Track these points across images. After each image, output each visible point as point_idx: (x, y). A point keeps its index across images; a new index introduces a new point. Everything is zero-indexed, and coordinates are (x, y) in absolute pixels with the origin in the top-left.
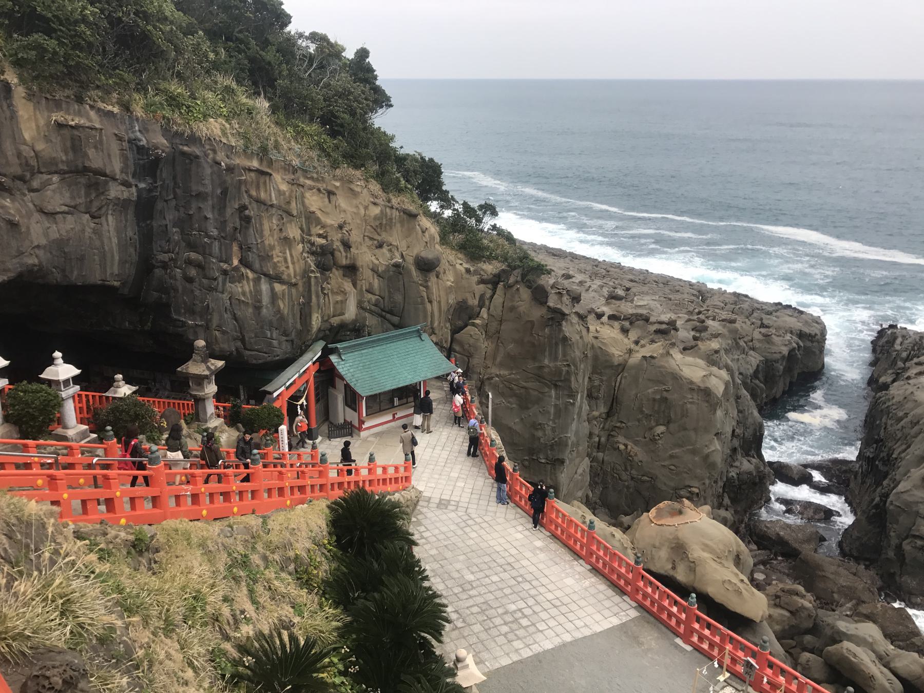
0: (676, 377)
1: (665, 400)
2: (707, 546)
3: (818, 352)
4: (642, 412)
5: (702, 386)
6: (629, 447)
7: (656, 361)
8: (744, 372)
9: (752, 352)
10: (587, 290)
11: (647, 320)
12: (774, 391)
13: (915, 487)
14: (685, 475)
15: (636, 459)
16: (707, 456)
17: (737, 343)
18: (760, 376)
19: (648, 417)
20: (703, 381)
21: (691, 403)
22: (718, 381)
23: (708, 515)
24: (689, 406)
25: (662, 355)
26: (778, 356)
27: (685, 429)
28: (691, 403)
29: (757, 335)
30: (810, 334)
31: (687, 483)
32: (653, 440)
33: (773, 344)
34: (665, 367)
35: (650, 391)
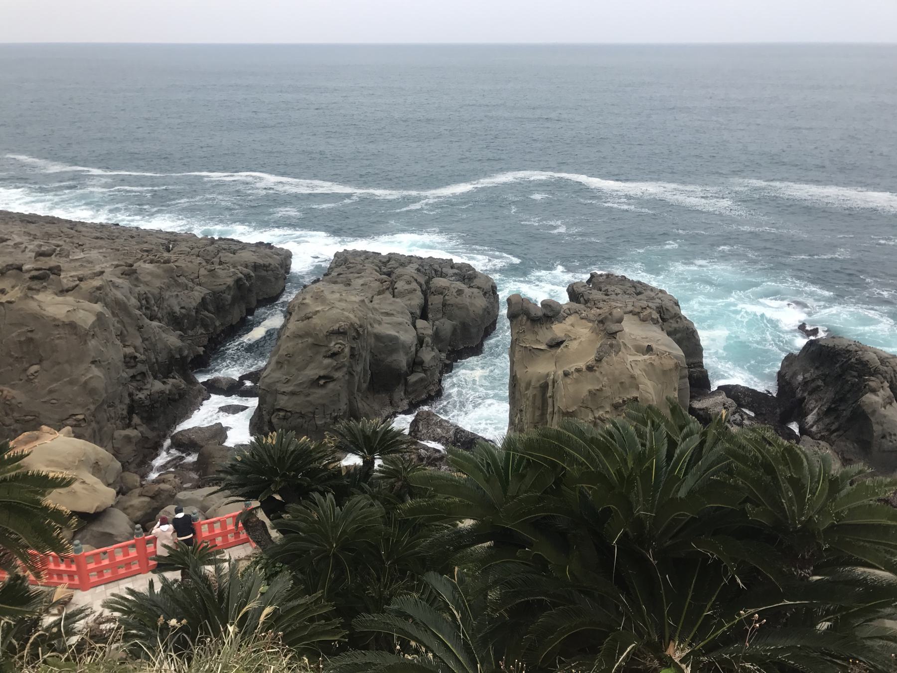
0: (37, 317)
1: (30, 340)
2: (52, 461)
3: (273, 280)
4: (11, 356)
5: (66, 320)
6: (5, 393)
7: (14, 305)
8: (186, 306)
9: (198, 288)
10: (23, 251)
11: (19, 268)
12: (228, 319)
13: (273, 371)
14: (67, 405)
15: (13, 401)
16: (86, 383)
17: (176, 281)
18: (211, 308)
19: (17, 359)
20: (67, 316)
21: (58, 338)
22: (86, 314)
23: (68, 435)
24: (57, 341)
25: (20, 299)
26: (224, 287)
27: (59, 363)
28: (58, 338)
29: (203, 272)
30: (264, 265)
31: (71, 412)
32: (29, 380)
33: (218, 277)
34: (21, 309)
35: (13, 335)
